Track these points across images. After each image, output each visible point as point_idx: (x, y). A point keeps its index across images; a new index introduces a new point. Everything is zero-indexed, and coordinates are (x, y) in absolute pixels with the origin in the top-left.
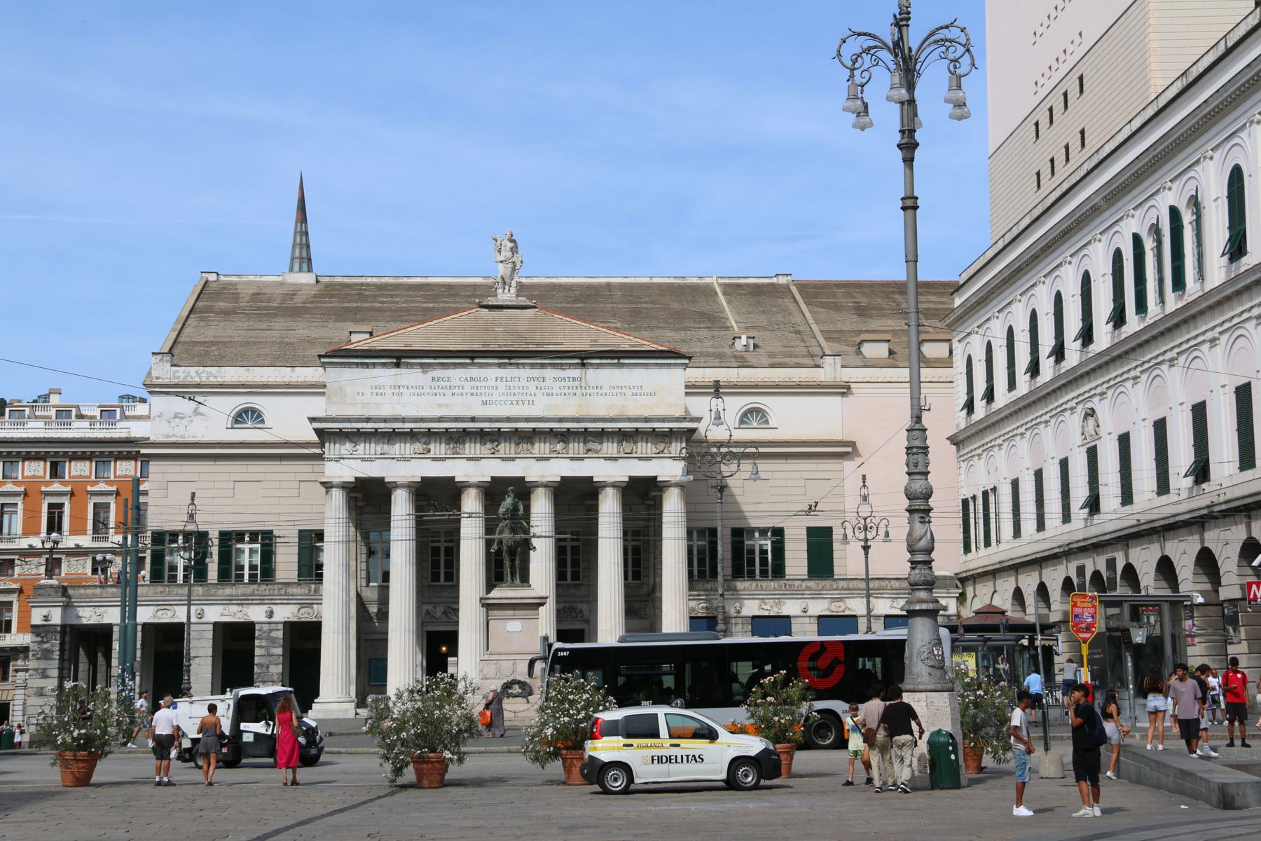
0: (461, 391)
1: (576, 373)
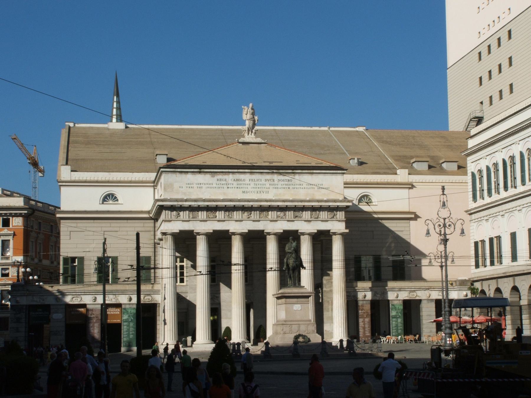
0: (232, 186)
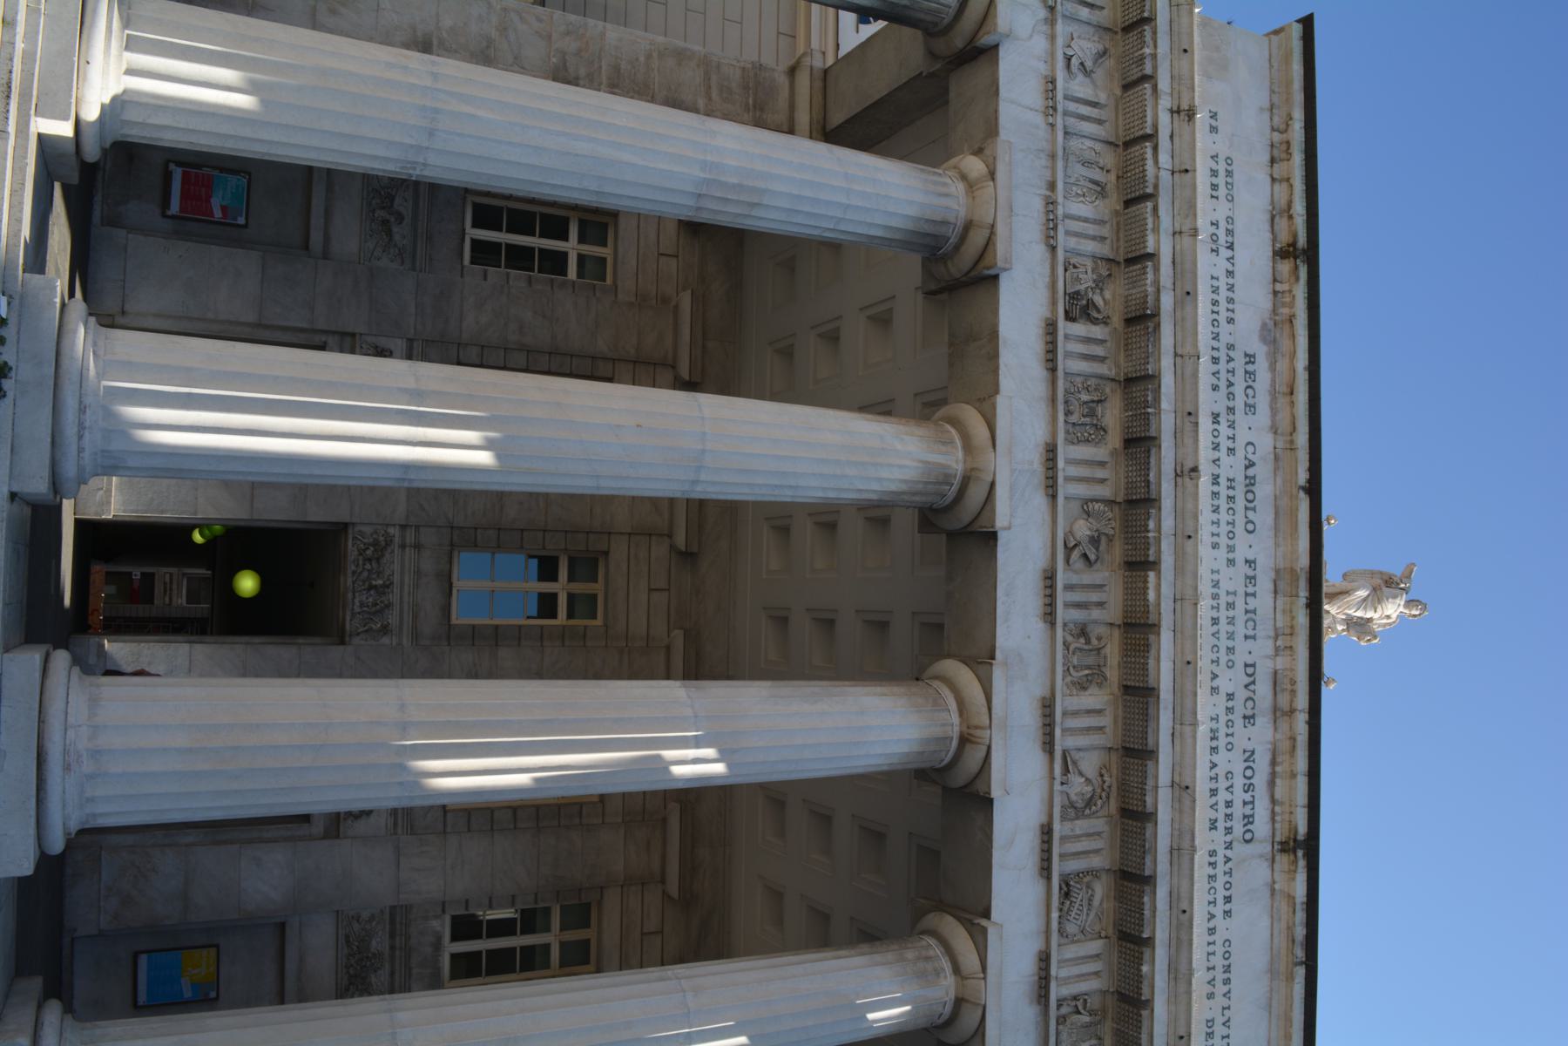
0: (1225, 444)
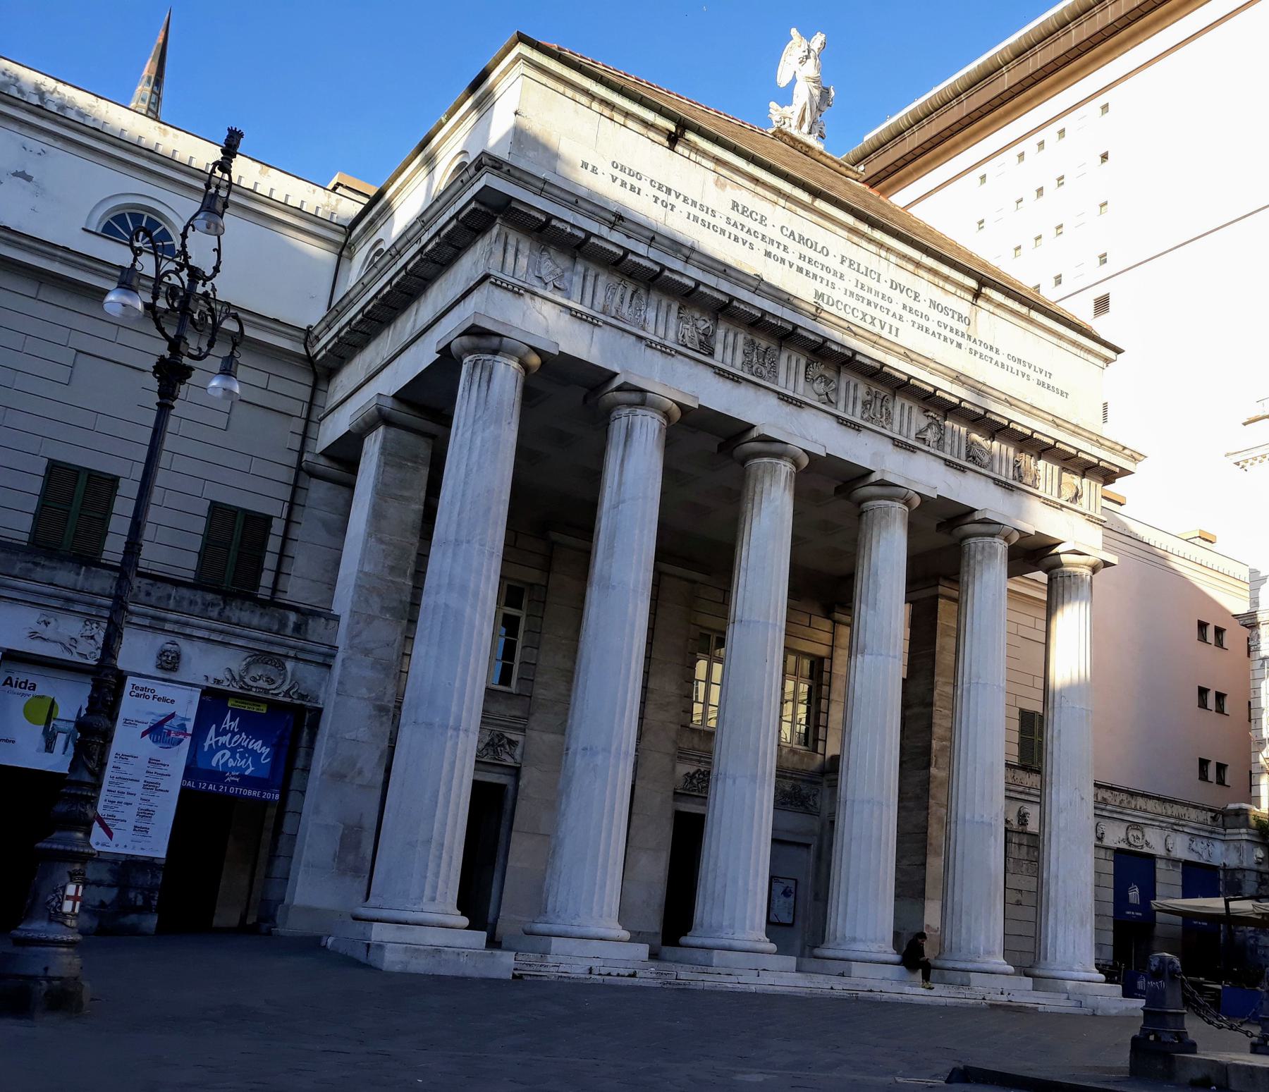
1: (962, 305)
